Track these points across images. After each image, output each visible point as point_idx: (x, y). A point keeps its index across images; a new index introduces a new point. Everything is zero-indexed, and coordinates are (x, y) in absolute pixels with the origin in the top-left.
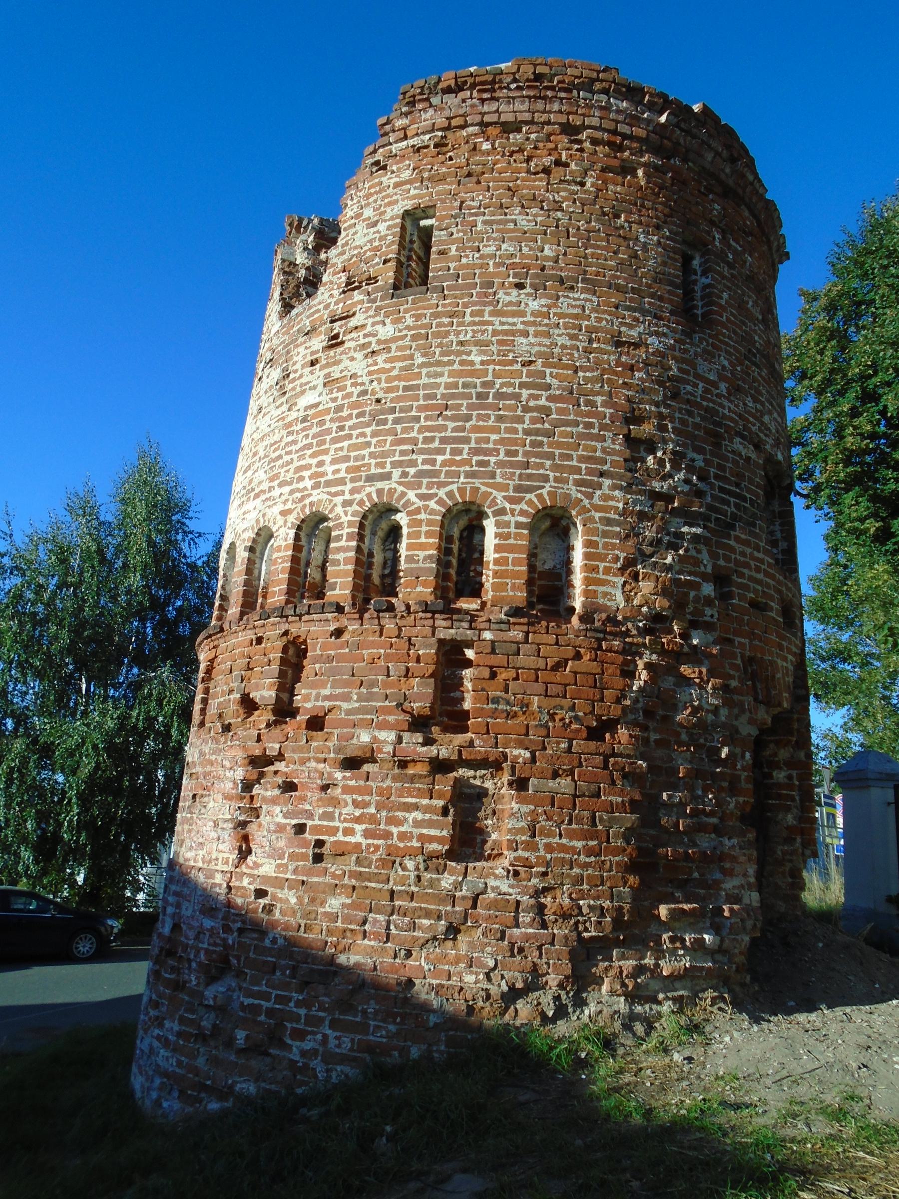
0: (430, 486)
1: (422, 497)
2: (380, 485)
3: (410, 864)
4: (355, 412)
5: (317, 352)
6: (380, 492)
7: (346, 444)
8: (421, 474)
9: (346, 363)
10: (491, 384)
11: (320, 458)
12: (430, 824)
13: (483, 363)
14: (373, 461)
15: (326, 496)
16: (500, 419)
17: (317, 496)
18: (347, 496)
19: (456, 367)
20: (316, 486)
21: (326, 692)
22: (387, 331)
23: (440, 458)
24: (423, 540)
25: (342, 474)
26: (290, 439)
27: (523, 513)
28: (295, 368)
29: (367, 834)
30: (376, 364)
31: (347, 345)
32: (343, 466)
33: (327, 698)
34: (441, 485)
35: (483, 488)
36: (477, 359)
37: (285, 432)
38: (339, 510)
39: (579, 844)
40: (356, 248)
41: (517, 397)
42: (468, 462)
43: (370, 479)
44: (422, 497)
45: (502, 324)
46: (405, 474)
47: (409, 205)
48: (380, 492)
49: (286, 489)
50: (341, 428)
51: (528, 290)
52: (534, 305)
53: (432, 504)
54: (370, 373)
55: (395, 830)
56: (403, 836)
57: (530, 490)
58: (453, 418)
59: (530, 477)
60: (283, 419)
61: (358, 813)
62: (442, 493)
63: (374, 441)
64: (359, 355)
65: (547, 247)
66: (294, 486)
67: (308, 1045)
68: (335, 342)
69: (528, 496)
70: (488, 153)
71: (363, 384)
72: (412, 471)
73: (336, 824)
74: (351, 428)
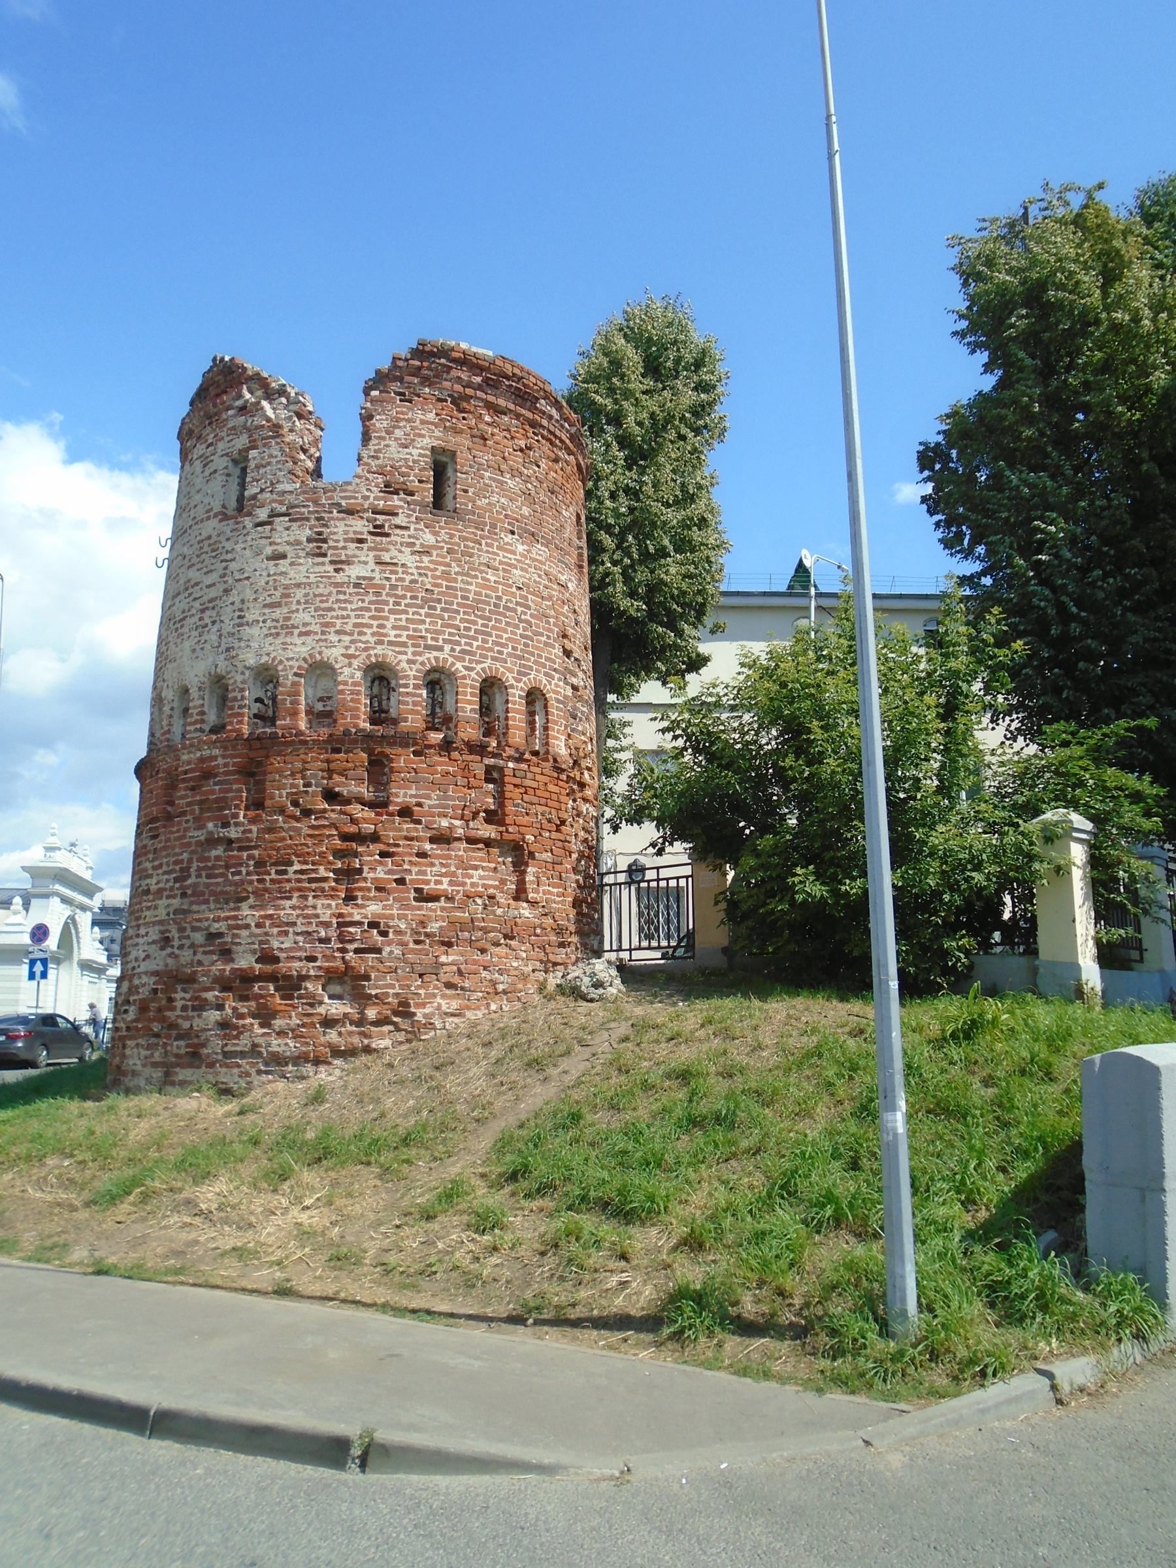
0: (471, 661)
1: (466, 668)
2: (435, 654)
3: (479, 901)
4: (409, 595)
5: (362, 533)
6: (437, 659)
7: (404, 617)
8: (463, 651)
9: (394, 553)
10: (499, 598)
11: (380, 622)
12: (490, 878)
13: (495, 582)
14: (429, 636)
15: (390, 653)
16: (507, 624)
17: (379, 650)
18: (410, 656)
19: (480, 581)
20: (380, 642)
21: (413, 792)
22: (429, 538)
23: (475, 644)
24: (469, 697)
25: (404, 639)
26: (342, 597)
27: (522, 689)
28: (335, 537)
29: (451, 883)
30: (421, 562)
31: (392, 538)
32: (405, 633)
33: (412, 796)
34: (478, 662)
35: (502, 669)
36: (493, 579)
37: (334, 591)
38: (404, 665)
39: (555, 890)
40: (389, 459)
41: (515, 611)
42: (491, 650)
43: (427, 647)
44: (466, 668)
45: (504, 557)
46: (453, 650)
47: (436, 443)
48: (437, 659)
49: (347, 638)
50: (399, 604)
51: (516, 536)
52: (521, 548)
53: (473, 674)
54: (417, 568)
55: (468, 881)
56: (473, 885)
57: (525, 674)
58: (481, 617)
59: (524, 666)
60: (329, 577)
61: (444, 870)
62: (479, 667)
63: (428, 620)
64: (407, 550)
65: (524, 508)
66: (356, 637)
67: (427, 1011)
68: (379, 531)
69: (524, 679)
70: (488, 424)
71: (412, 574)
72: (458, 648)
73: (429, 877)
74: (406, 605)
